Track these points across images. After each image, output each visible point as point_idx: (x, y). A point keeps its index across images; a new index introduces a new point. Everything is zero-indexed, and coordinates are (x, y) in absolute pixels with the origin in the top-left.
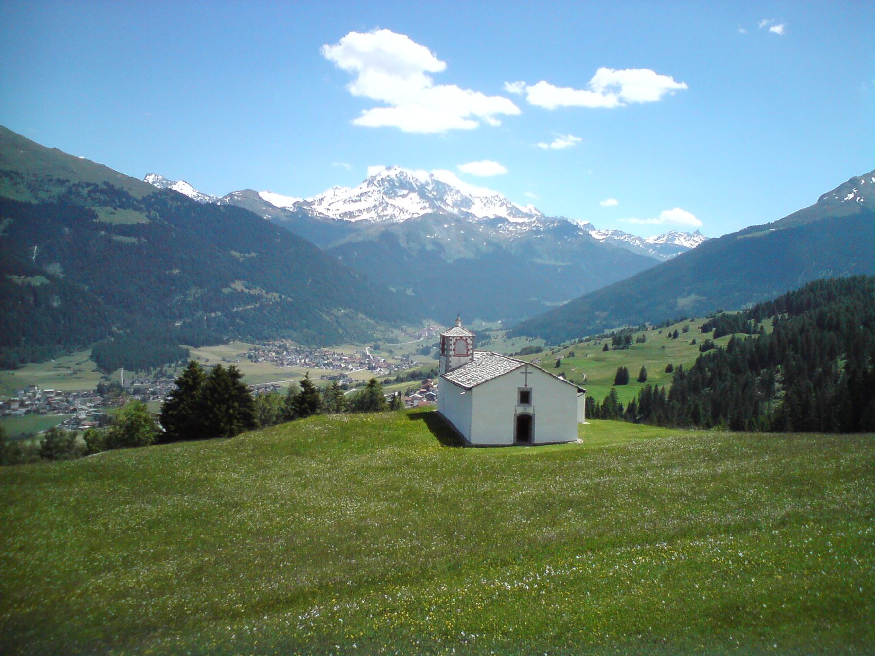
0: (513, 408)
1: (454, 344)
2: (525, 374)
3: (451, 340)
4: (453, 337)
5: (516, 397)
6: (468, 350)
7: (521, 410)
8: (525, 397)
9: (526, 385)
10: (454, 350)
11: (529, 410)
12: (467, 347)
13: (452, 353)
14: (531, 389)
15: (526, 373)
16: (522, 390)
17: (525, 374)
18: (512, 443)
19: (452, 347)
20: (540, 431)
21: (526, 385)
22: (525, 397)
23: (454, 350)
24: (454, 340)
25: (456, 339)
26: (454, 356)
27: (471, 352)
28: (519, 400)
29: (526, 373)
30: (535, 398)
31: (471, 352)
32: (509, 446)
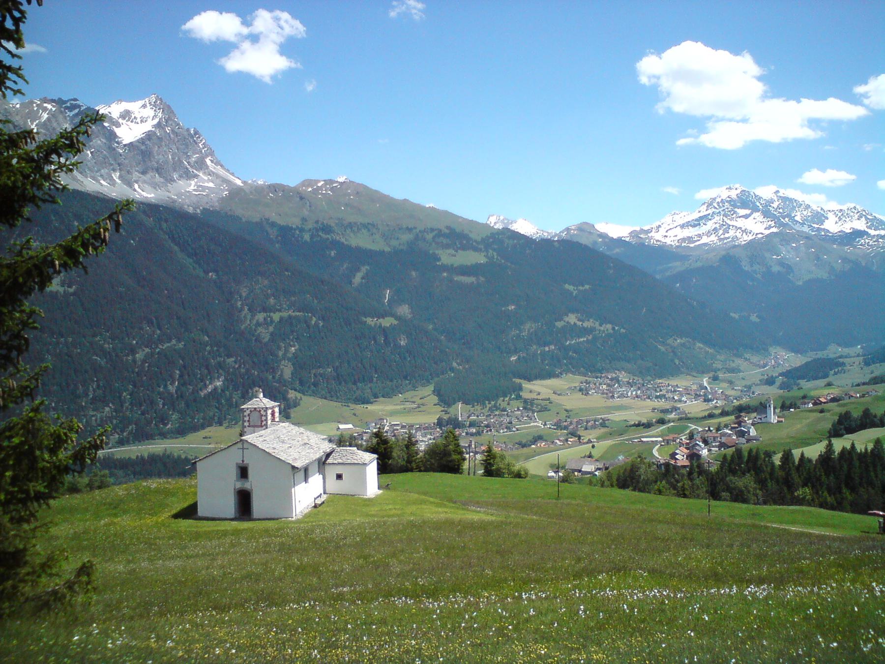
0: (231, 483)
1: (249, 415)
2: (245, 450)
3: (245, 411)
4: (248, 409)
5: (234, 472)
6: (262, 421)
7: (239, 485)
8: (243, 472)
9: (243, 461)
10: (249, 421)
11: (247, 486)
12: (261, 418)
13: (246, 424)
14: (248, 464)
15: (243, 449)
16: (240, 465)
17: (245, 450)
18: (232, 516)
19: (247, 419)
20: (258, 506)
21: (243, 461)
22: (243, 472)
23: (249, 421)
24: (248, 412)
25: (251, 411)
26: (248, 426)
27: (265, 423)
28: (239, 475)
29: (243, 449)
30: (251, 472)
31: (265, 423)
32: (226, 519)
